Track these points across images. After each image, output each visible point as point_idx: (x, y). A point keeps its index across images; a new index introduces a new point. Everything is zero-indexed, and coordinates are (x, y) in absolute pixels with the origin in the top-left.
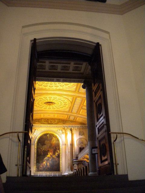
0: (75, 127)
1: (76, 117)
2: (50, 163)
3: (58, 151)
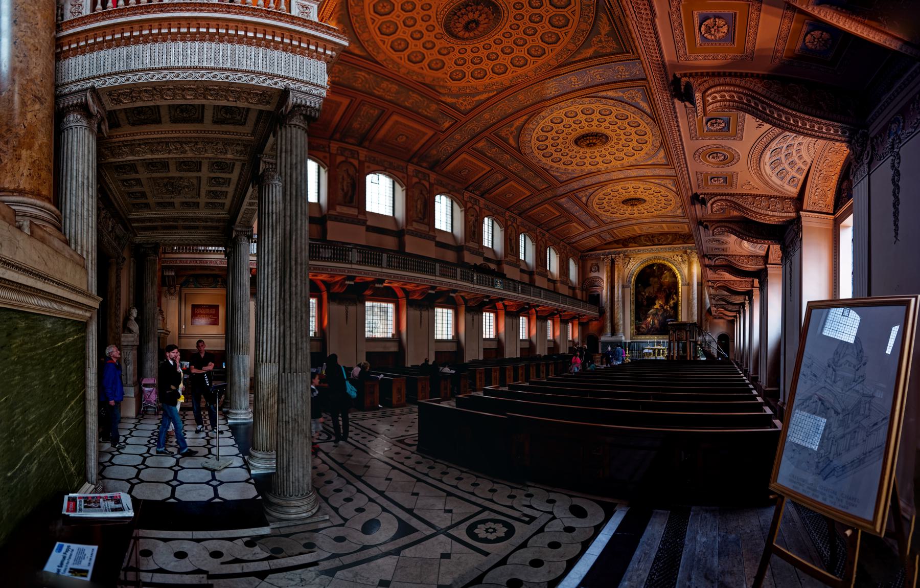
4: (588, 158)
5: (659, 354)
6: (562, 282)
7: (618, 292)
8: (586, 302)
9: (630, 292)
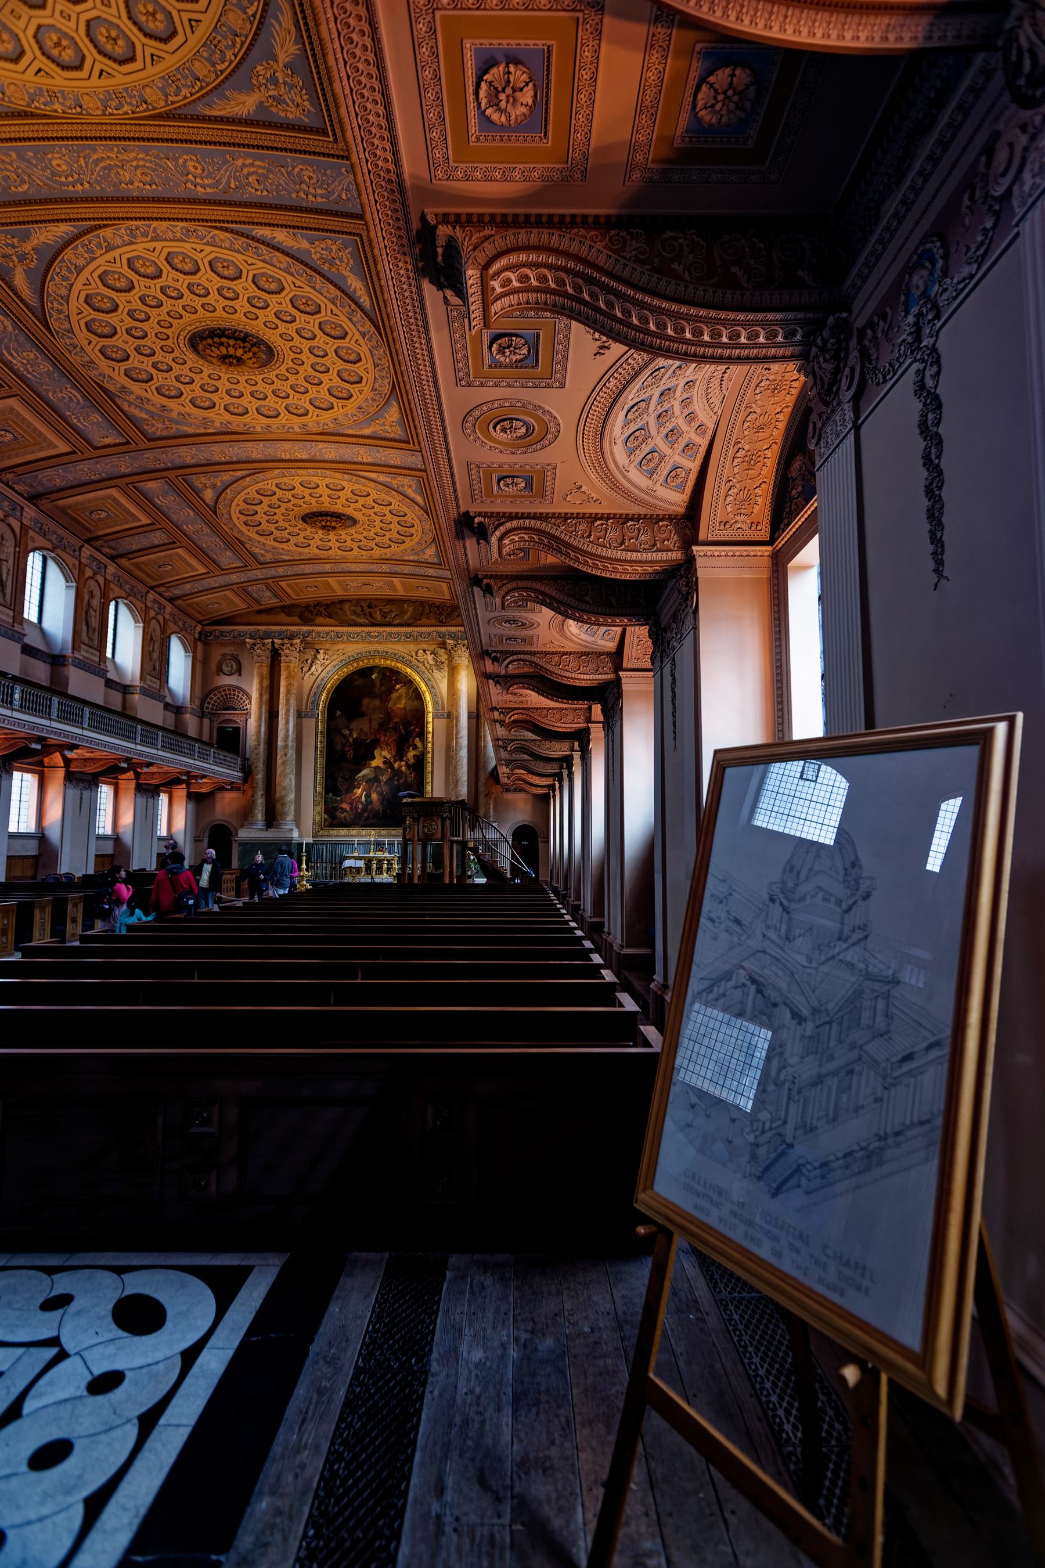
2: (380, 794)
4: (222, 393)
5: (379, 870)
6: (145, 692)
7: (286, 725)
8: (210, 745)
9: (315, 727)
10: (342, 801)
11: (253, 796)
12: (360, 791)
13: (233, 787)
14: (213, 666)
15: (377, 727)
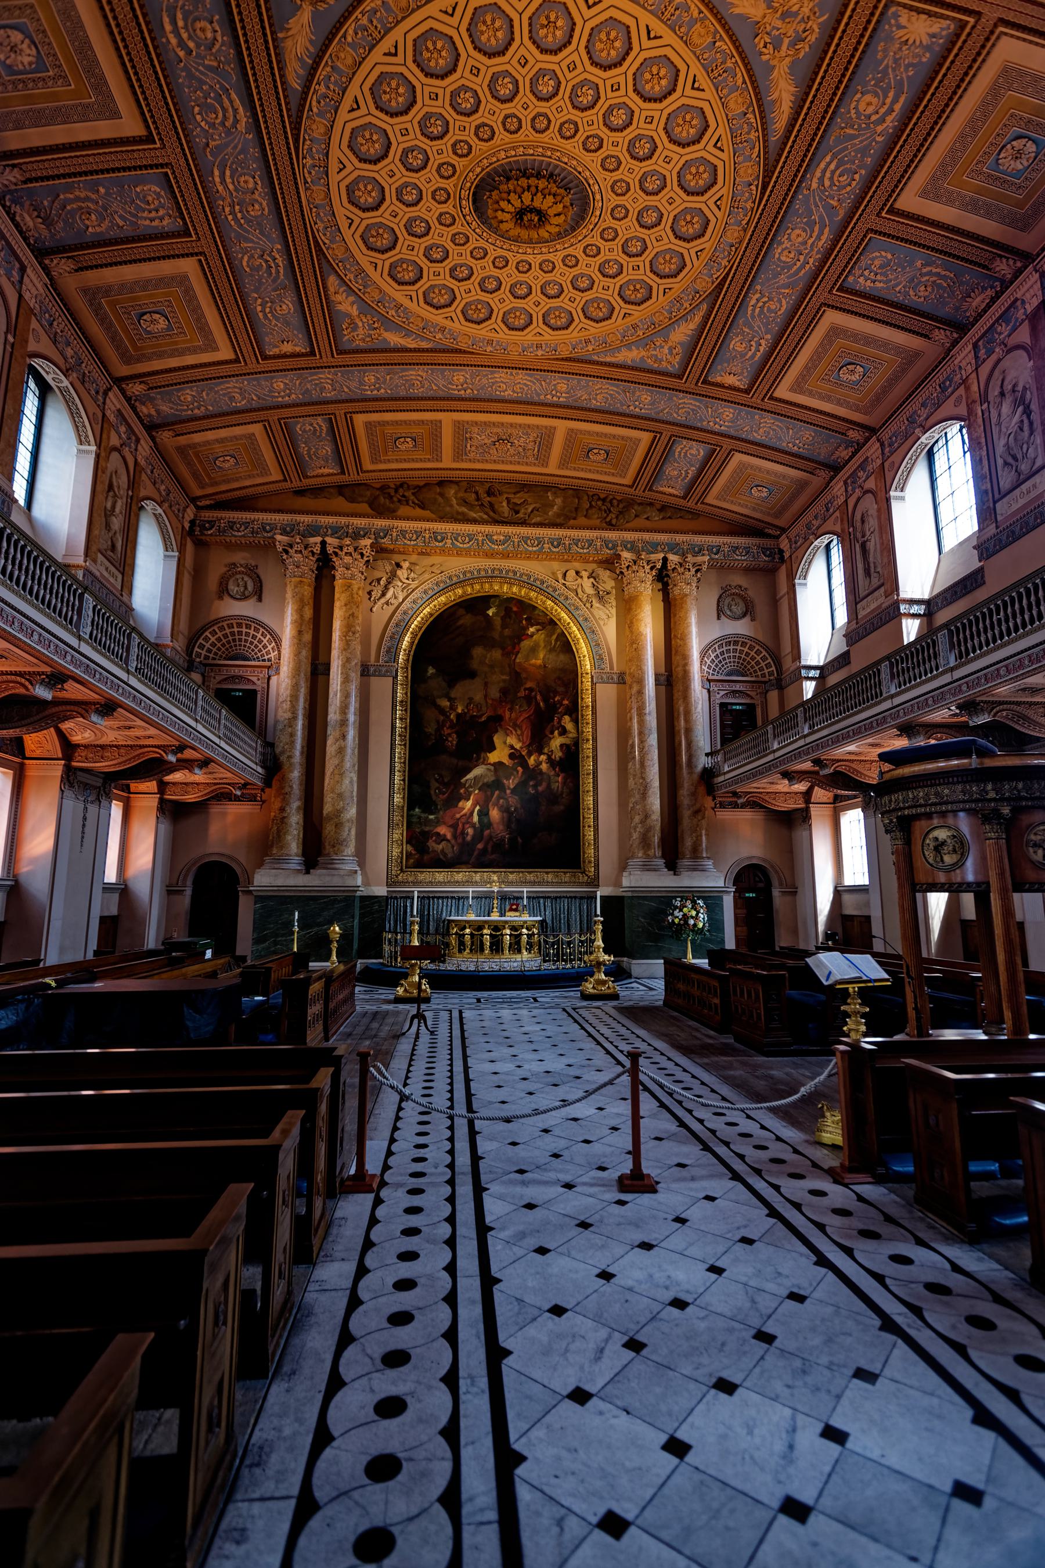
0: (699, 551)
1: (727, 444)
2: (505, 810)
3: (567, 722)
10: (438, 822)
11: (282, 810)
12: (469, 804)
13: (246, 793)
14: (212, 582)
15: (498, 695)
